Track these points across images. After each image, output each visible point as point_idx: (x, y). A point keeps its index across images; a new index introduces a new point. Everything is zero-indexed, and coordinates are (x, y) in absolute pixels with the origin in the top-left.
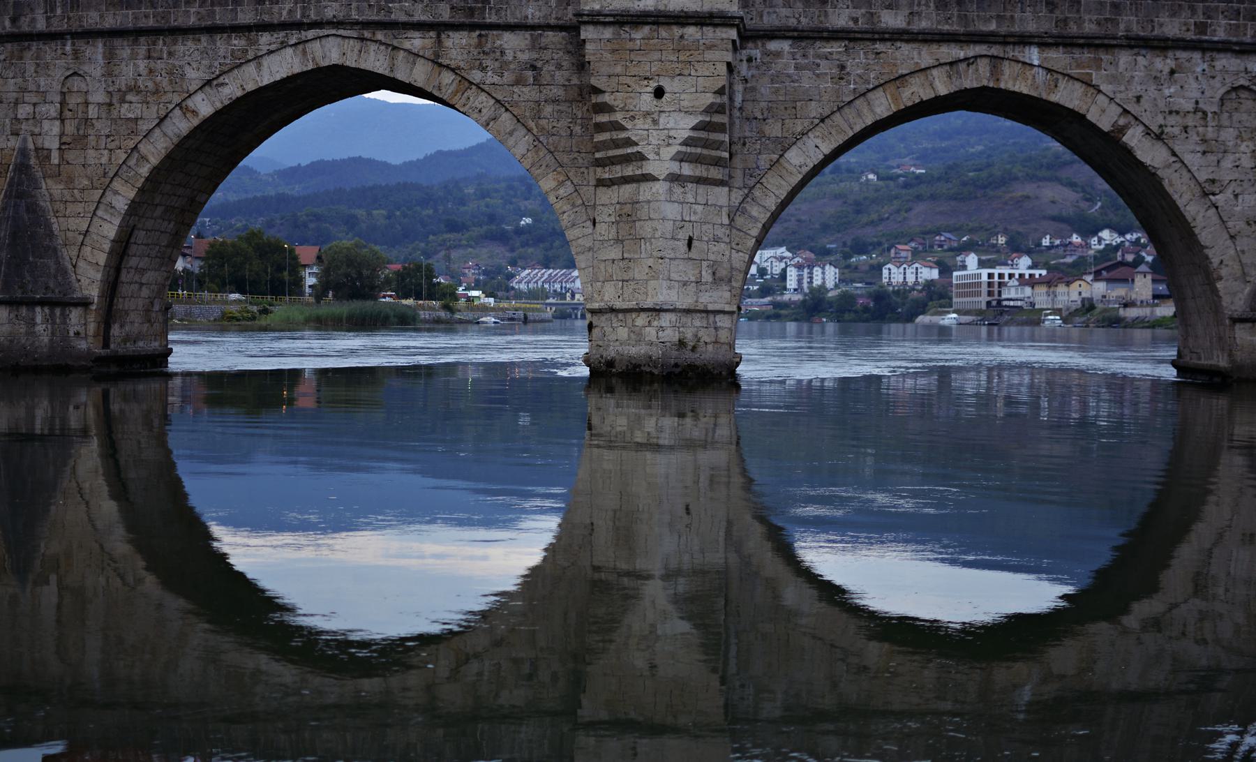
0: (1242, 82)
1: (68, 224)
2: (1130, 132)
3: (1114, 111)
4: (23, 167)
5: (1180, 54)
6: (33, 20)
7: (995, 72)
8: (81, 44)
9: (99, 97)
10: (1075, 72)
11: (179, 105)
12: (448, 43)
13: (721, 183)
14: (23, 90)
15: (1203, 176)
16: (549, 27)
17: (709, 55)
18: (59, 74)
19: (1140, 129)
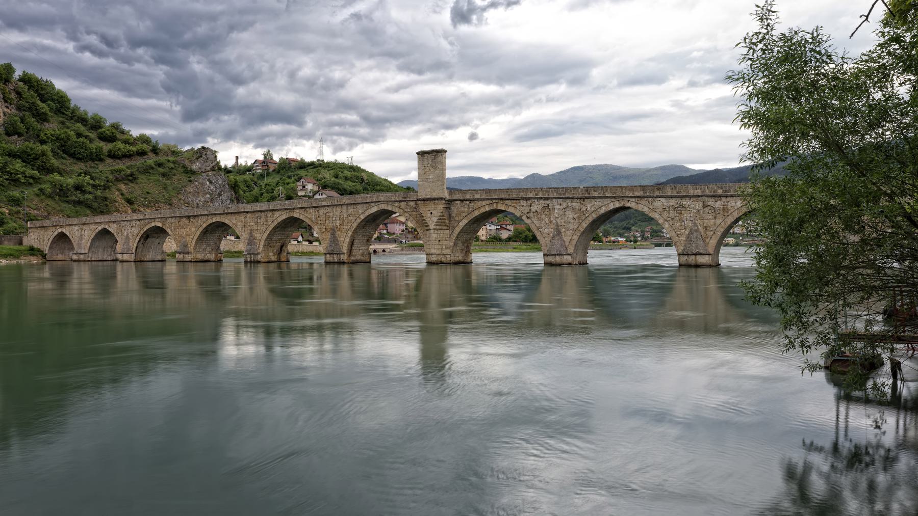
1: (341, 239)
7: (497, 205)
13: (447, 229)
18: (339, 212)
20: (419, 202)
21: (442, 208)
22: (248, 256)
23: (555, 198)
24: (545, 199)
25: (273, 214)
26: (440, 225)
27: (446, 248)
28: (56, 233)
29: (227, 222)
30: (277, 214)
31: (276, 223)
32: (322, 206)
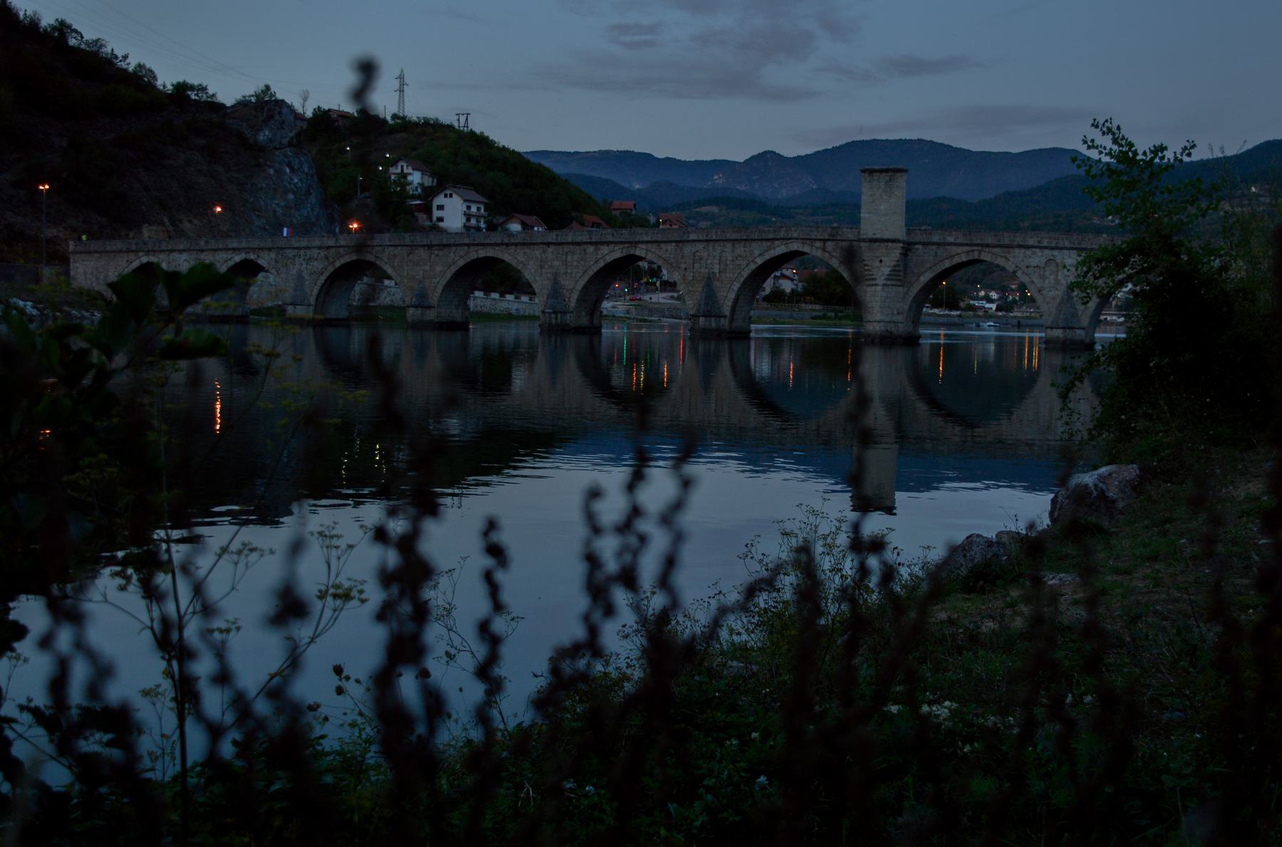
0: (1052, 258)
2: (1018, 272)
3: (1013, 266)
4: (709, 278)
5: (1034, 250)
6: (712, 236)
7: (980, 254)
8: (725, 243)
9: (730, 258)
10: (1002, 255)
11: (752, 261)
12: (827, 245)
13: (901, 286)
14: (709, 255)
15: (1039, 285)
16: (855, 241)
17: (895, 251)
18: (719, 251)
19: (1021, 272)
20: (862, 244)
21: (898, 255)
22: (553, 316)
23: (1066, 248)
24: (1052, 249)
25: (596, 250)
26: (893, 279)
27: (898, 313)
28: (136, 264)
29: (506, 257)
30: (605, 249)
31: (602, 264)
32: (688, 241)
